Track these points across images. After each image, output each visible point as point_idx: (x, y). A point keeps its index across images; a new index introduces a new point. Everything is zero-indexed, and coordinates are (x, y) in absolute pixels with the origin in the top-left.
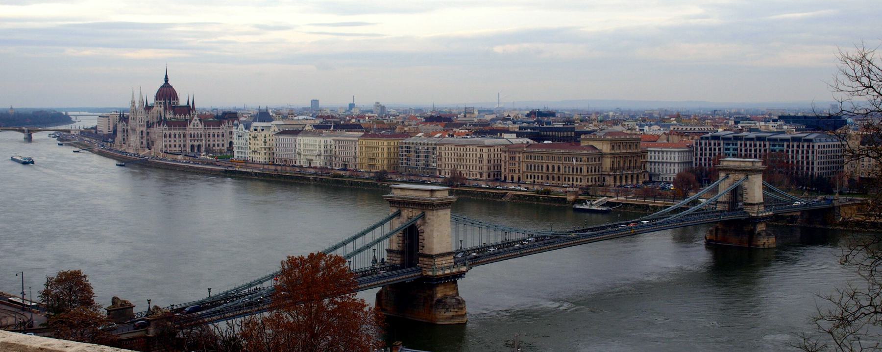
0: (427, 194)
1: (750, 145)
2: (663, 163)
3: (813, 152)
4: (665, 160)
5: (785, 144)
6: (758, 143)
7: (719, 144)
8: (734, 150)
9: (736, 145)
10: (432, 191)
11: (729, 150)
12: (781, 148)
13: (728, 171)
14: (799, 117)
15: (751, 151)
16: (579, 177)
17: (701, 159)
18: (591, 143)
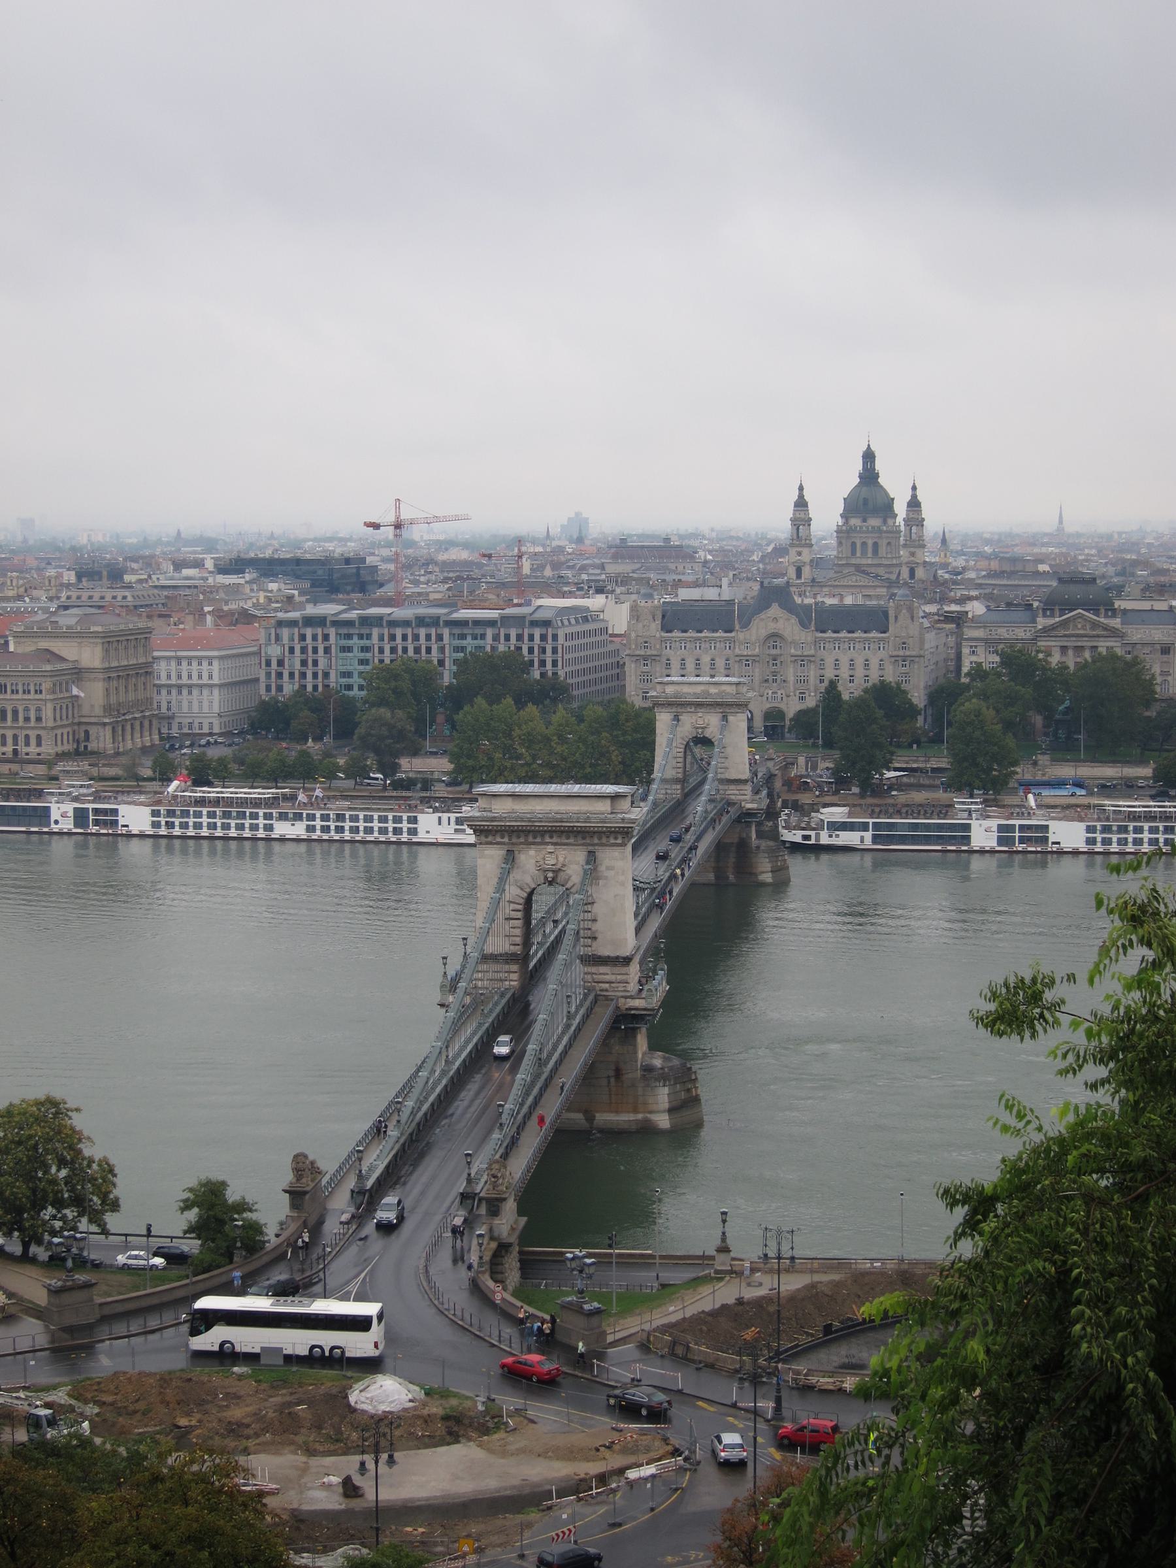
0: (604, 807)
1: (405, 638)
2: (180, 688)
3: (555, 651)
4: (185, 680)
5: (489, 632)
6: (422, 632)
7: (326, 637)
8: (365, 649)
9: (369, 636)
10: (615, 797)
11: (349, 649)
12: (479, 642)
13: (678, 706)
14: (283, 562)
15: (405, 650)
16: (33, 735)
17: (280, 675)
18: (44, 644)
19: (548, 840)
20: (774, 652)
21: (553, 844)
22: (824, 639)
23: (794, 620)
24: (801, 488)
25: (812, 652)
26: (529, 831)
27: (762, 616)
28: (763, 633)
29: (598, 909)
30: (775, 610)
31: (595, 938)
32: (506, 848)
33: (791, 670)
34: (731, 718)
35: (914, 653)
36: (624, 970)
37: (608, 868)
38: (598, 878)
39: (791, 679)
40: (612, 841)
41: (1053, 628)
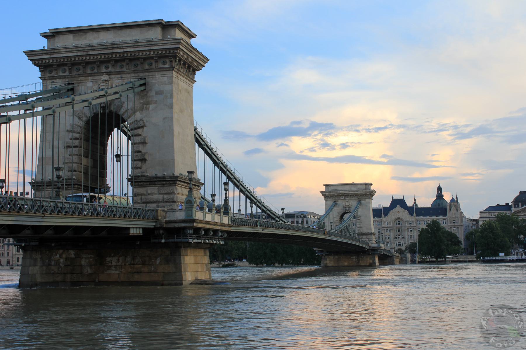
19: (104, 70)
20: (399, 226)
21: (109, 73)
22: (419, 220)
23: (407, 212)
24: (415, 200)
25: (415, 225)
26: (87, 63)
27: (393, 211)
28: (394, 218)
29: (147, 133)
30: (398, 208)
31: (144, 160)
32: (67, 81)
33: (406, 233)
34: (363, 202)
35: (458, 224)
36: (169, 189)
37: (158, 93)
38: (148, 103)
39: (406, 237)
40: (161, 66)
41: (519, 212)
